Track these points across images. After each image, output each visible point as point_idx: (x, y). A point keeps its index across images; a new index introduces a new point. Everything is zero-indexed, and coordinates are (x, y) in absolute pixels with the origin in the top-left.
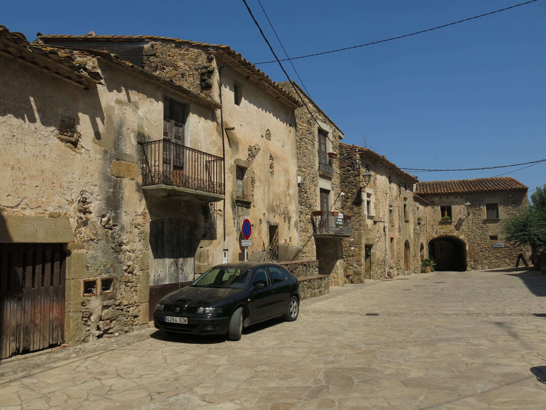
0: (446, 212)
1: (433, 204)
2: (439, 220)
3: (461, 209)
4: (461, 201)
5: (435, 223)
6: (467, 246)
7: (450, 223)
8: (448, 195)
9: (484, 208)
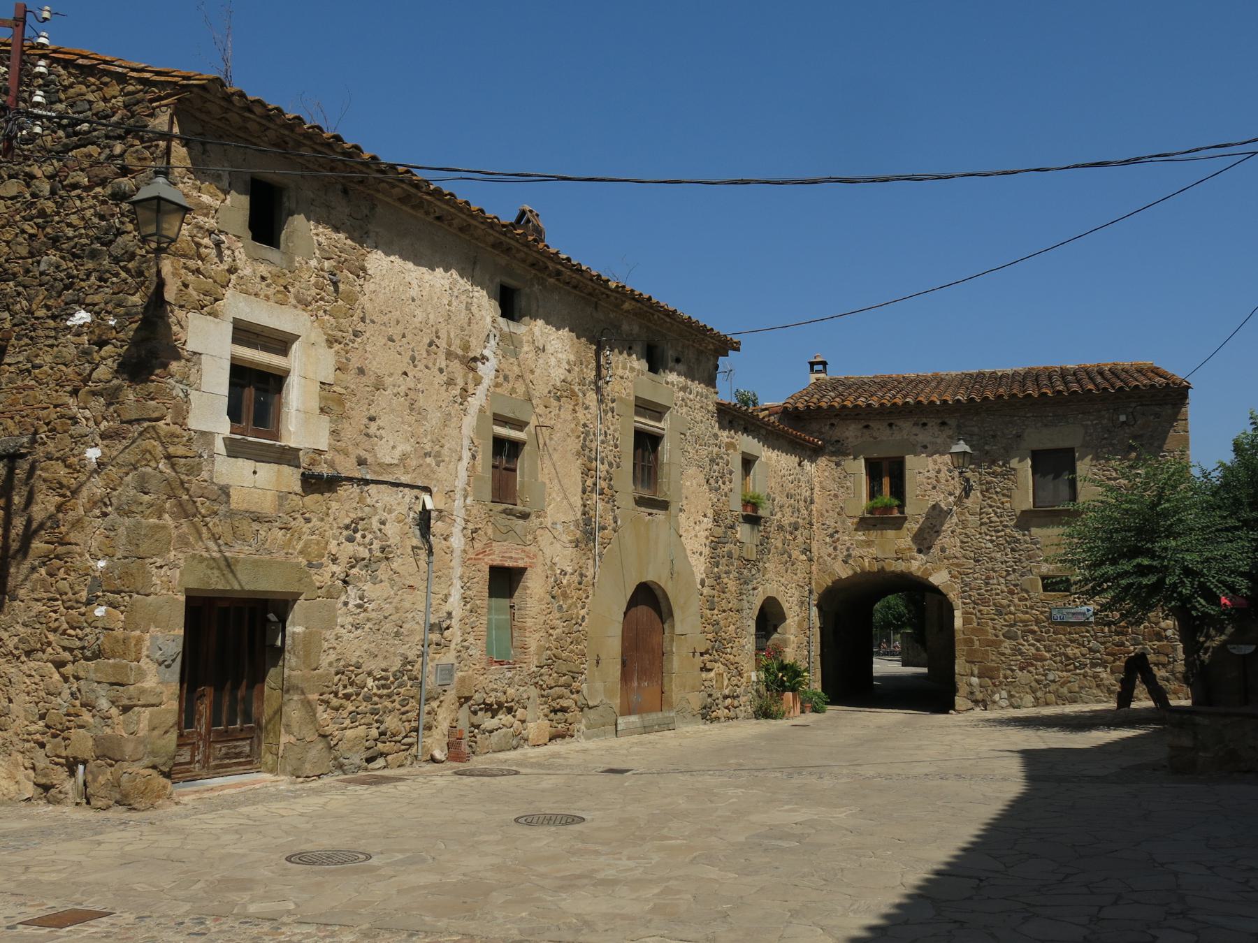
0: (886, 482)
1: (838, 450)
2: (859, 513)
3: (939, 472)
4: (939, 441)
5: (843, 522)
6: (958, 614)
7: (898, 524)
8: (892, 414)
9: (1024, 468)
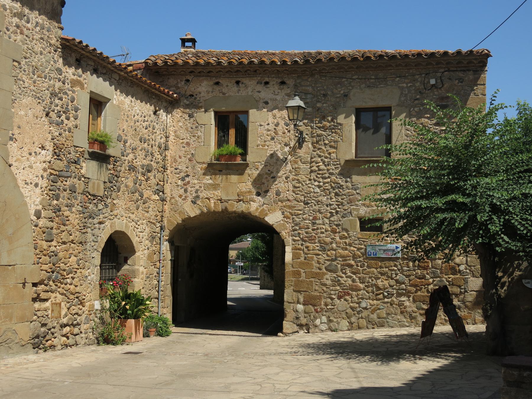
0: (232, 132)
2: (208, 160)
3: (277, 125)
4: (279, 98)
5: (193, 167)
6: (288, 250)
7: (240, 170)
